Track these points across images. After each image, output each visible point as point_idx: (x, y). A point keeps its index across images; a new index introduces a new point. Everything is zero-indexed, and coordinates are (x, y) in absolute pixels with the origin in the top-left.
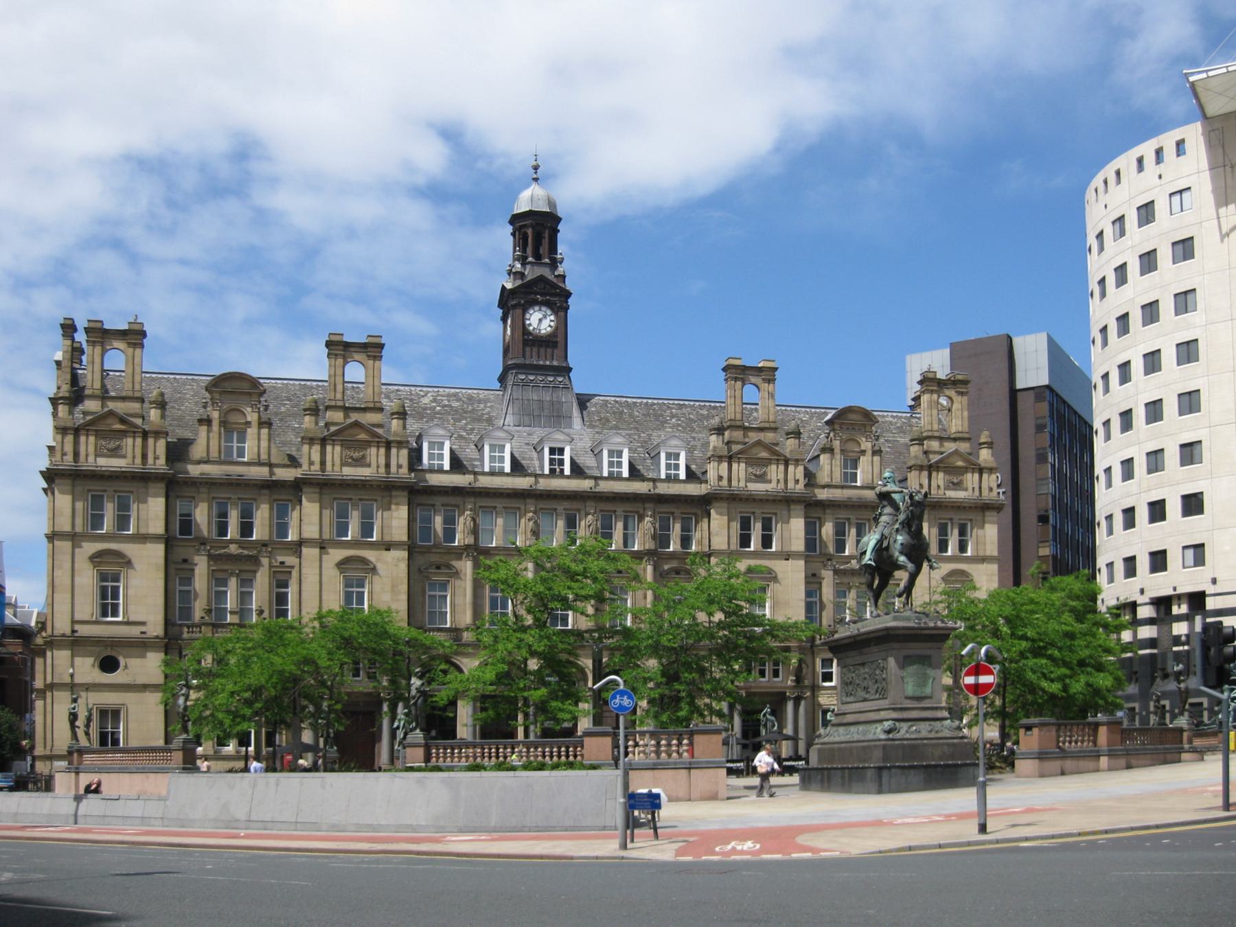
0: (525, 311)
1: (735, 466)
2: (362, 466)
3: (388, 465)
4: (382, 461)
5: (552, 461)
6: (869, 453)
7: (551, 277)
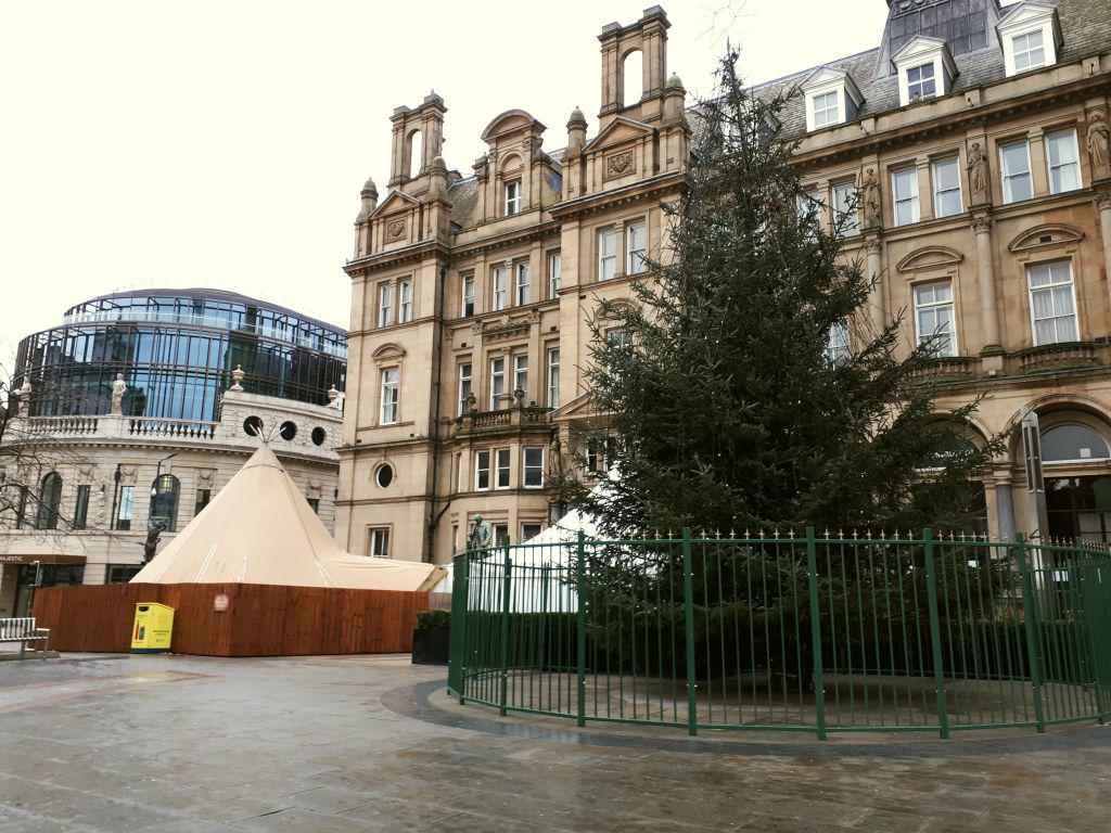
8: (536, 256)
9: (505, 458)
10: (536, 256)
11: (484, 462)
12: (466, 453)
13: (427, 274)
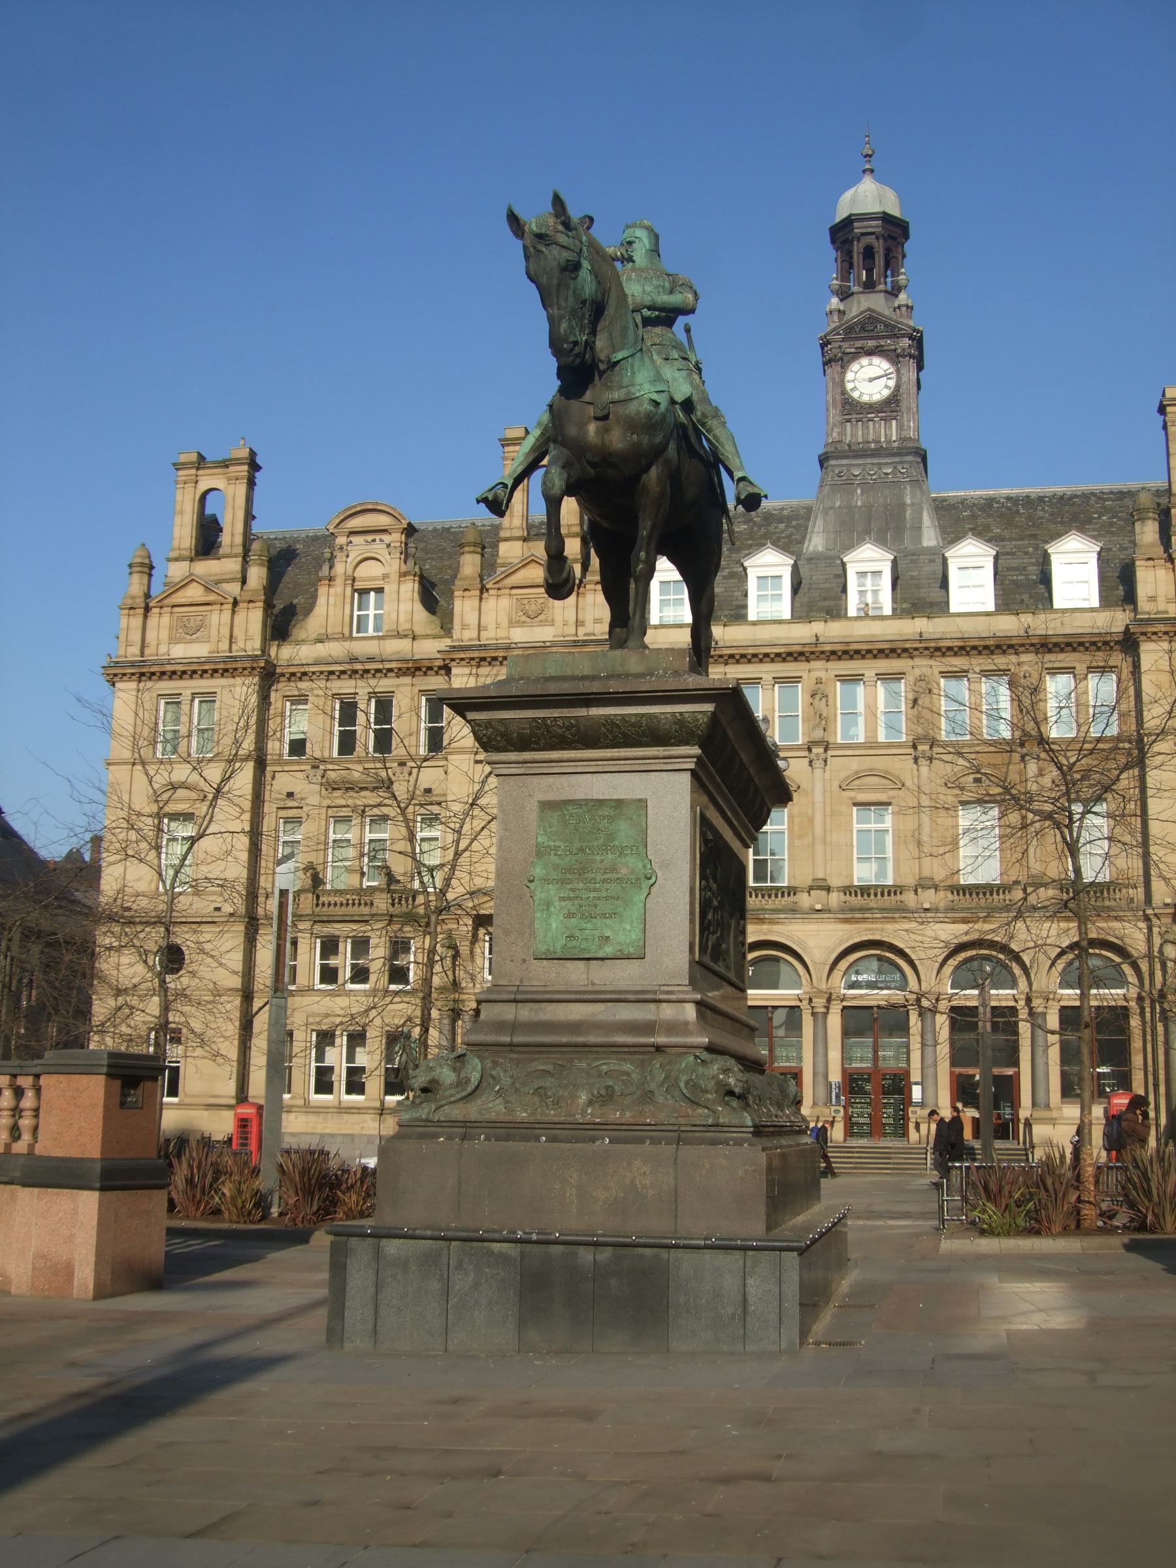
0: (844, 368)
2: (543, 623)
3: (578, 623)
7: (887, 312)
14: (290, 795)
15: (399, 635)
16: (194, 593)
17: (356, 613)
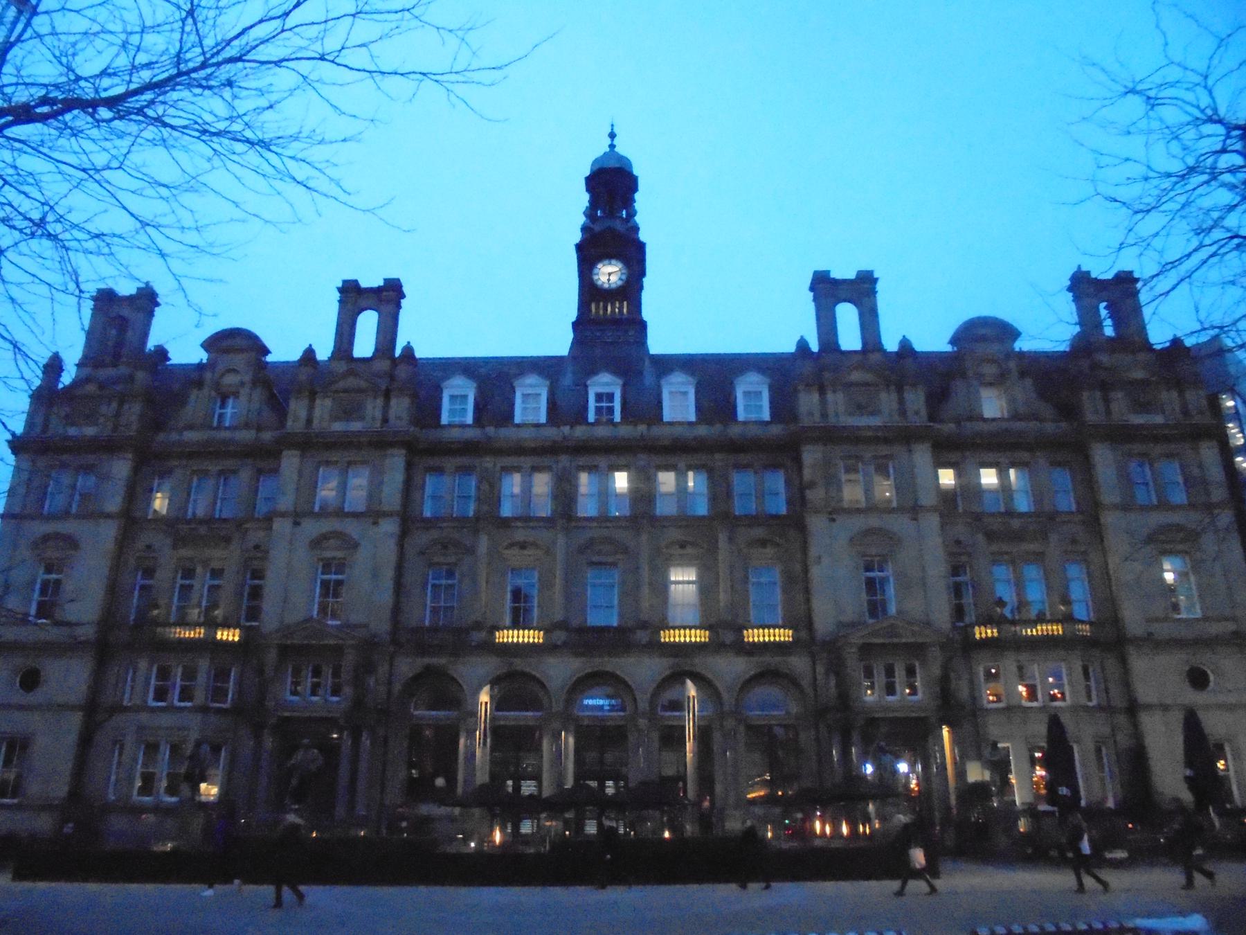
1: (830, 396)
3: (385, 420)
4: (378, 414)
5: (599, 410)
6: (1015, 374)
8: (245, 475)
9: (190, 674)
10: (245, 475)
11: (164, 674)
12: (143, 664)
13: (396, 462)
14: (149, 547)
15: (247, 426)
16: (91, 388)
17: (218, 411)
